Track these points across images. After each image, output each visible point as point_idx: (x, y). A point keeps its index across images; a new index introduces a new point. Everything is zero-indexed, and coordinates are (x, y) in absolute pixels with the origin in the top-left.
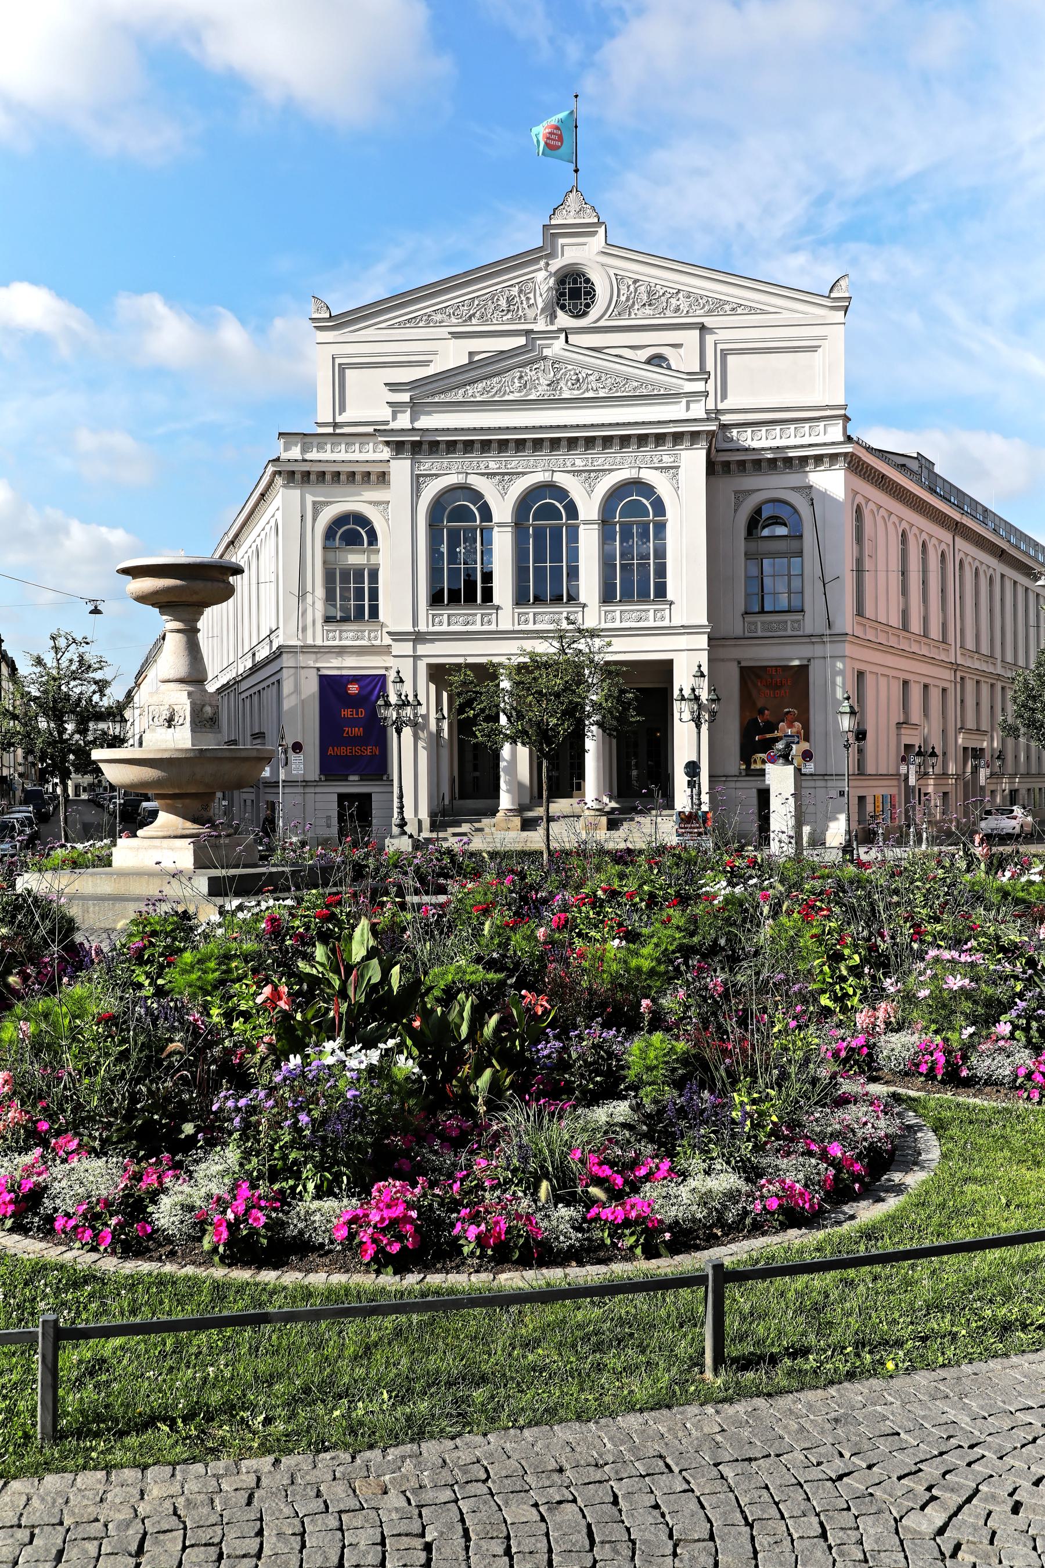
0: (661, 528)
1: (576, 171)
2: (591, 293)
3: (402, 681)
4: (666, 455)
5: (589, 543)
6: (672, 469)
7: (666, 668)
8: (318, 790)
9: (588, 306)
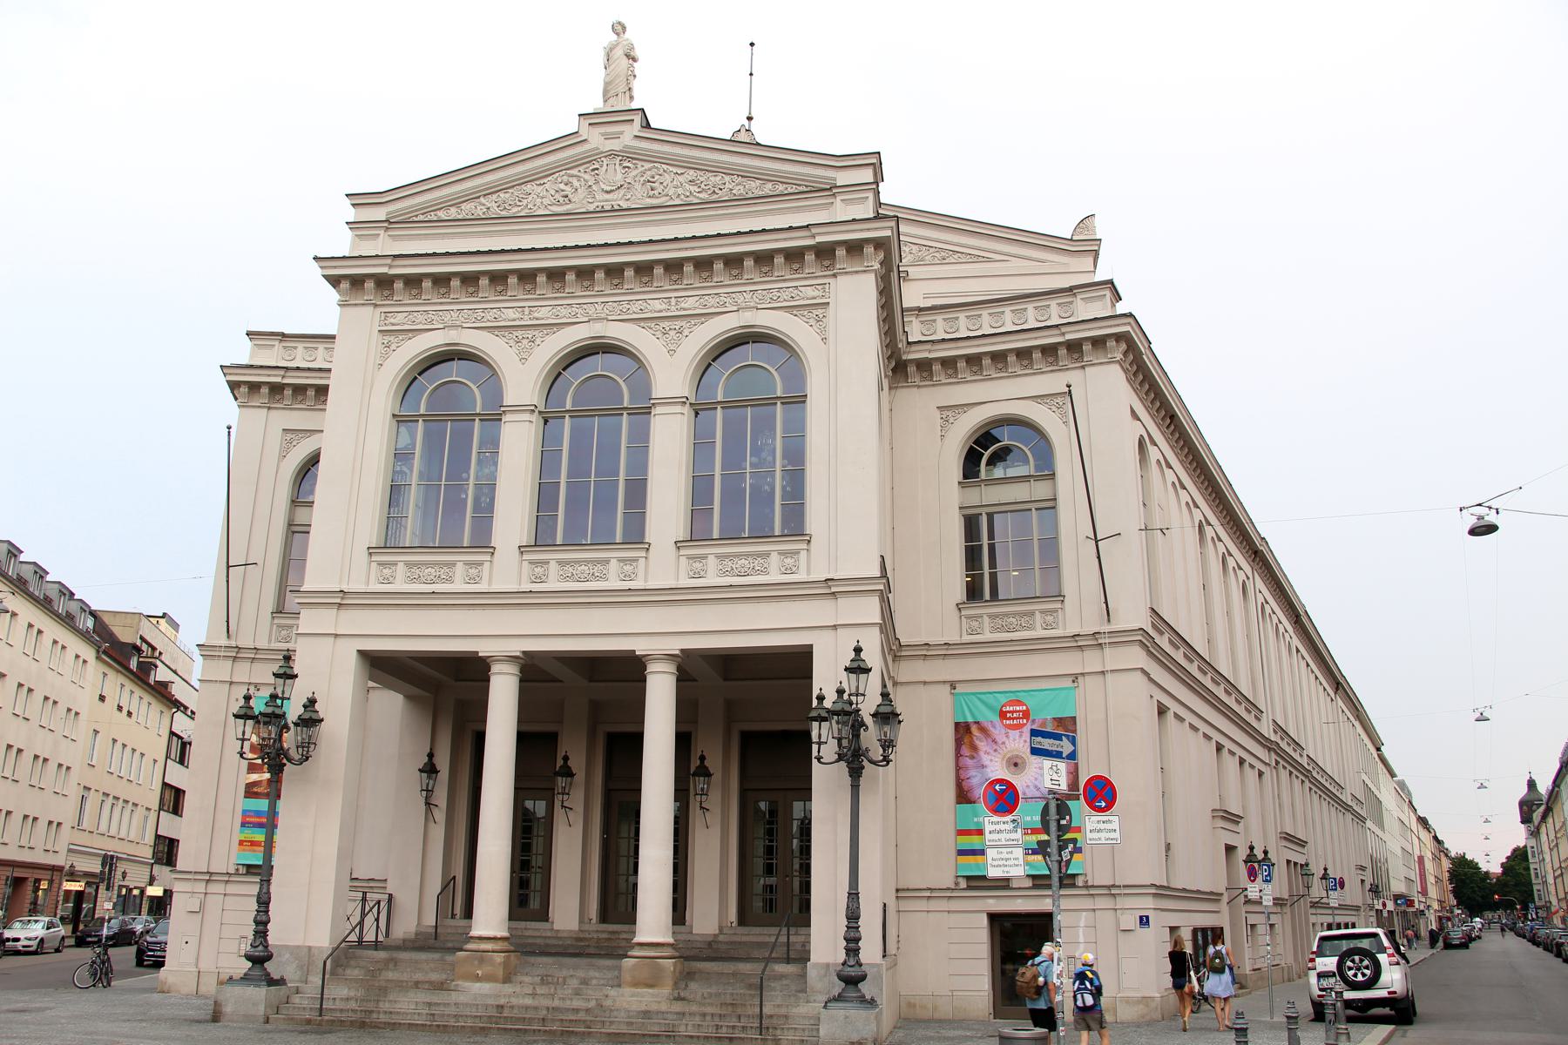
5: (670, 437)
7: (798, 662)
8: (231, 889)
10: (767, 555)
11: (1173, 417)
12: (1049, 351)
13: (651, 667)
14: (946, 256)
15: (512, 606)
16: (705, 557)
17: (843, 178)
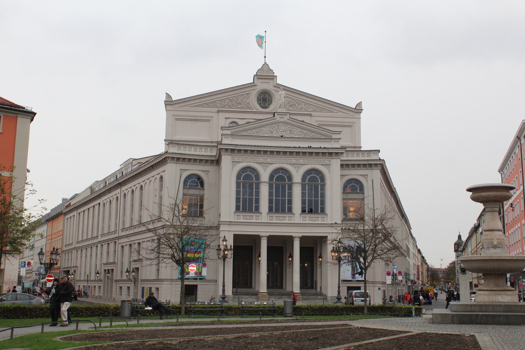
0: (323, 186)
1: (265, 57)
2: (259, 100)
3: (226, 241)
4: (326, 160)
6: (328, 165)
9: (269, 105)
10: (318, 217)
11: (385, 173)
12: (365, 165)
13: (295, 239)
14: (322, 110)
15: (264, 224)
16: (306, 217)
17: (334, 136)
